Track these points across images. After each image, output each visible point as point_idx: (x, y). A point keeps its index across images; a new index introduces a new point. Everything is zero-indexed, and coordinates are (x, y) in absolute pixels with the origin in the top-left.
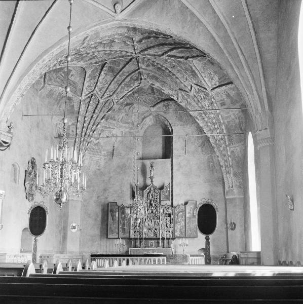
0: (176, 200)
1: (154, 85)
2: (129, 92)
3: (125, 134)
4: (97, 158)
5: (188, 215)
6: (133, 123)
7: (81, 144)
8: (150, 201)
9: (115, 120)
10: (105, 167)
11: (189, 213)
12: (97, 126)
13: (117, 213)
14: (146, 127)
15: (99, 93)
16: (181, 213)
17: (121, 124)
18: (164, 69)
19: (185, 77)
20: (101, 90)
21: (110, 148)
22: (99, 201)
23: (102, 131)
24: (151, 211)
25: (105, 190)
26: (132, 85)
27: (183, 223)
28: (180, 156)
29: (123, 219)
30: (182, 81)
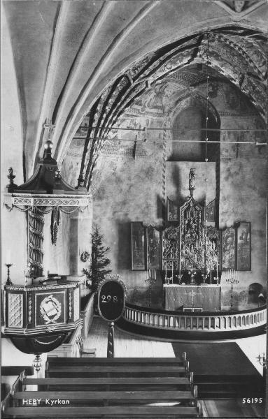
0: (222, 220)
1: (210, 63)
2: (172, 71)
3: (152, 123)
4: (112, 158)
5: (239, 241)
6: (163, 108)
7: (96, 142)
8: (189, 221)
9: (141, 105)
10: (123, 170)
11: (241, 238)
12: (118, 116)
13: (143, 237)
14: (179, 112)
15: (132, 73)
16: (230, 238)
17: (147, 109)
18: (232, 45)
19: (263, 60)
20: (137, 69)
21: (130, 144)
22: (117, 218)
23: (124, 120)
24: (189, 235)
25: (124, 203)
26: (178, 62)
27: (233, 252)
28: (230, 159)
29: (152, 245)
30: (257, 66)
